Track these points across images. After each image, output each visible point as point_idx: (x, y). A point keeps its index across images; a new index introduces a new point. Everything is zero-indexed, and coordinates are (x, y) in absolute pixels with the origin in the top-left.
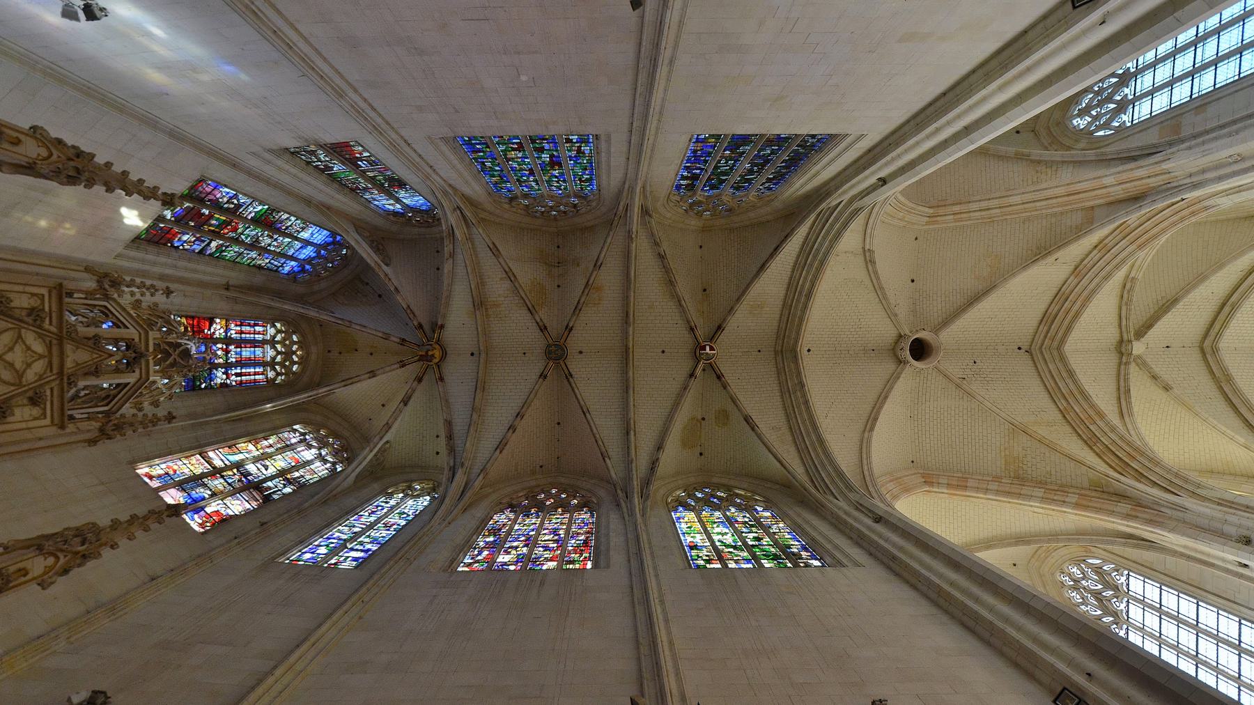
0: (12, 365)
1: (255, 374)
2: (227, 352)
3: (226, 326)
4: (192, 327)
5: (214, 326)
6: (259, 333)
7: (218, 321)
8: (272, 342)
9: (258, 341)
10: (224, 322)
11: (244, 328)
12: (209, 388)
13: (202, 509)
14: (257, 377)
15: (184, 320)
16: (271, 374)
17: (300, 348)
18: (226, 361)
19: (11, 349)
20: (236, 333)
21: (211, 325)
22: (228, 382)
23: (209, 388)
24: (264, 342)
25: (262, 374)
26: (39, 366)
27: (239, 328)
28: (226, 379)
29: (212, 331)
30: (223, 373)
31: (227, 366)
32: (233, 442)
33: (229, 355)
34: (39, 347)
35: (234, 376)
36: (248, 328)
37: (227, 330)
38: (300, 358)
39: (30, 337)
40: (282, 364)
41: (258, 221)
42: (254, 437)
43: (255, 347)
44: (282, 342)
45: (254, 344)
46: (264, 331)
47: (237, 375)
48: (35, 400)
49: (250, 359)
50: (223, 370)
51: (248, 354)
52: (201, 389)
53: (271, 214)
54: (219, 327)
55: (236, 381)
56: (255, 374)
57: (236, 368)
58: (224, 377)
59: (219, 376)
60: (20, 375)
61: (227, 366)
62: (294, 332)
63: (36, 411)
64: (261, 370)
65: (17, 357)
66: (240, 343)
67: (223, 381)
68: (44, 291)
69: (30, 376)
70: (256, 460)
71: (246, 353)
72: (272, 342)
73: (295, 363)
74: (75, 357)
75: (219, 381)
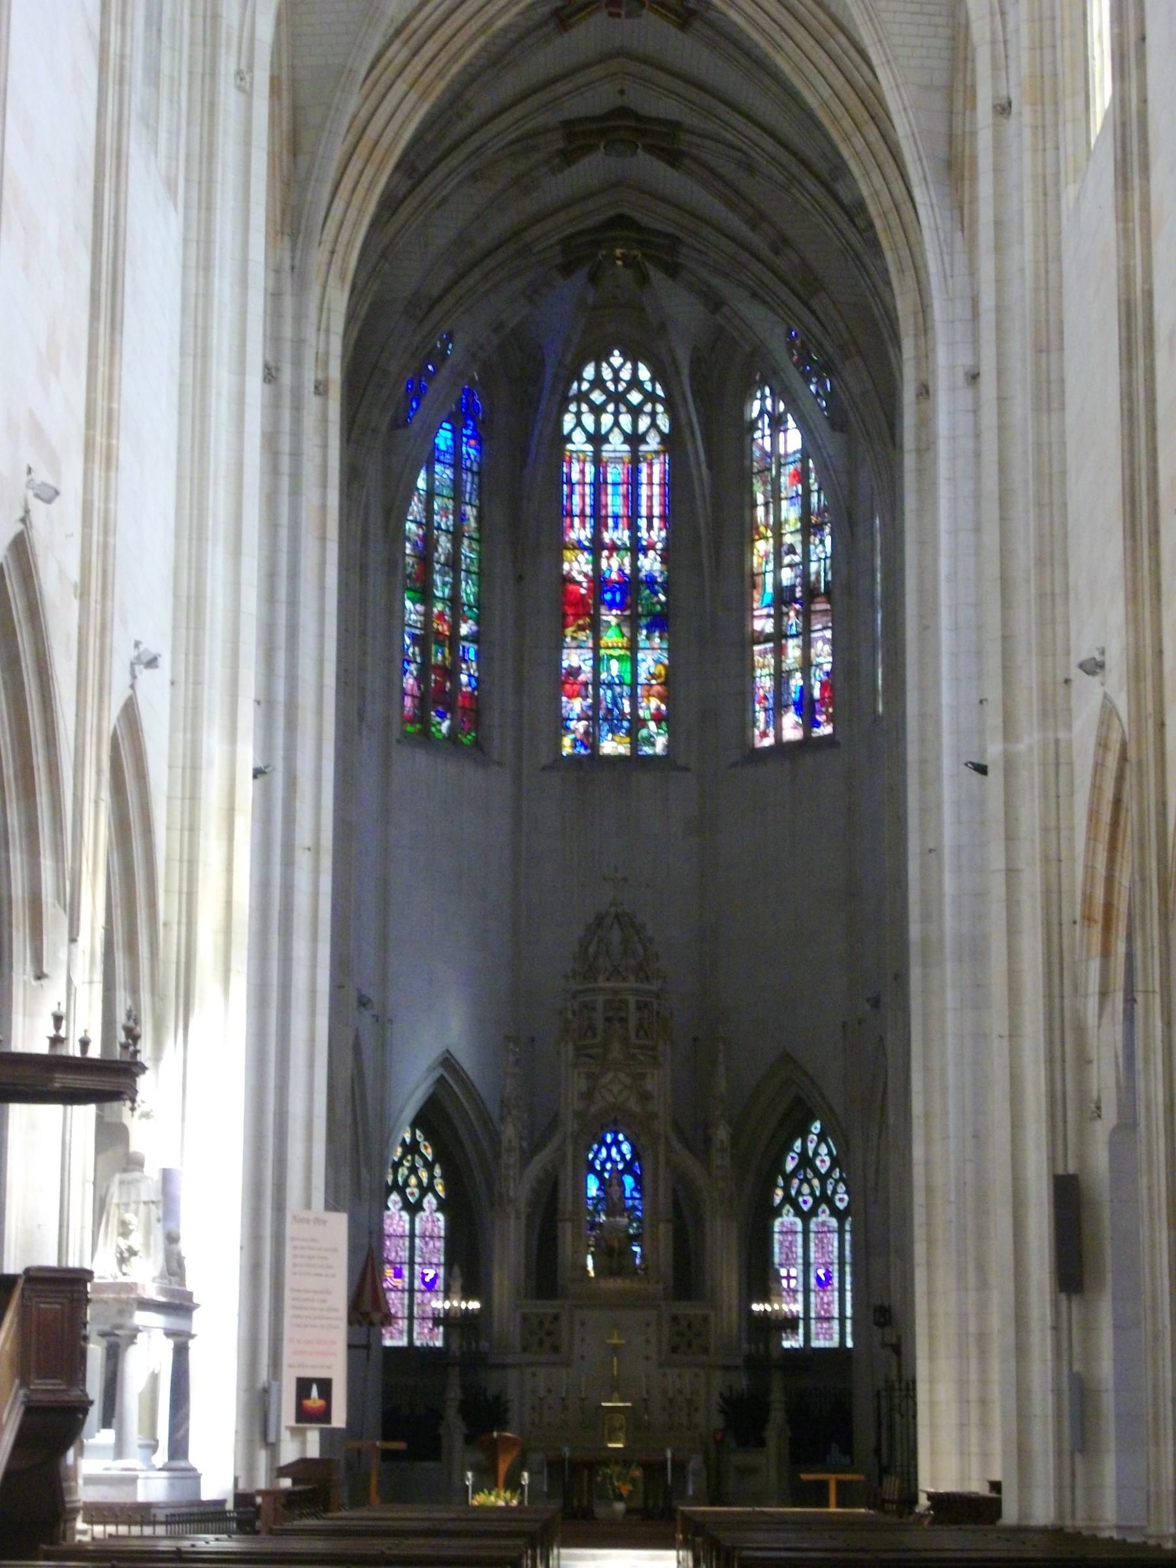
0: (620, 1092)
1: (650, 484)
2: (614, 548)
3: (574, 548)
4: (577, 616)
5: (574, 574)
6: (582, 472)
7: (566, 566)
8: (597, 439)
9: (597, 474)
10: (568, 554)
11: (576, 510)
12: (666, 587)
13: (813, 701)
15: (569, 631)
16: (653, 442)
17: (606, 356)
18: (626, 549)
19: (611, 1091)
20: (584, 528)
22: (659, 546)
23: (666, 587)
24: (597, 461)
25: (651, 465)
26: (621, 1075)
27: (577, 521)
28: (655, 550)
29: (580, 578)
30: (646, 556)
31: (637, 548)
32: (748, 580)
33: (619, 543)
34: (610, 1075)
35: (652, 533)
36: (576, 499)
37: (579, 546)
39: (604, 1081)
40: (635, 411)
41: (425, 596)
42: (749, 533)
43: (606, 482)
44: (597, 410)
45: (599, 485)
46: (578, 460)
47: (650, 527)
48: (643, 1076)
49: (625, 497)
50: (641, 556)
51: (619, 500)
52: (667, 603)
53: (409, 576)
54: (575, 565)
55: (660, 529)
56: (650, 484)
57: (638, 529)
58: (651, 553)
59: (650, 564)
60: (626, 1087)
61: (637, 548)
62: (580, 379)
63: (649, 1076)
64: (644, 467)
65: (616, 1089)
66: (599, 520)
67: (659, 559)
68: (576, 1071)
69: (628, 1081)
70: (779, 565)
71: (614, 503)
72: (597, 439)
73: (635, 370)
74: (616, 1052)
75: (657, 566)
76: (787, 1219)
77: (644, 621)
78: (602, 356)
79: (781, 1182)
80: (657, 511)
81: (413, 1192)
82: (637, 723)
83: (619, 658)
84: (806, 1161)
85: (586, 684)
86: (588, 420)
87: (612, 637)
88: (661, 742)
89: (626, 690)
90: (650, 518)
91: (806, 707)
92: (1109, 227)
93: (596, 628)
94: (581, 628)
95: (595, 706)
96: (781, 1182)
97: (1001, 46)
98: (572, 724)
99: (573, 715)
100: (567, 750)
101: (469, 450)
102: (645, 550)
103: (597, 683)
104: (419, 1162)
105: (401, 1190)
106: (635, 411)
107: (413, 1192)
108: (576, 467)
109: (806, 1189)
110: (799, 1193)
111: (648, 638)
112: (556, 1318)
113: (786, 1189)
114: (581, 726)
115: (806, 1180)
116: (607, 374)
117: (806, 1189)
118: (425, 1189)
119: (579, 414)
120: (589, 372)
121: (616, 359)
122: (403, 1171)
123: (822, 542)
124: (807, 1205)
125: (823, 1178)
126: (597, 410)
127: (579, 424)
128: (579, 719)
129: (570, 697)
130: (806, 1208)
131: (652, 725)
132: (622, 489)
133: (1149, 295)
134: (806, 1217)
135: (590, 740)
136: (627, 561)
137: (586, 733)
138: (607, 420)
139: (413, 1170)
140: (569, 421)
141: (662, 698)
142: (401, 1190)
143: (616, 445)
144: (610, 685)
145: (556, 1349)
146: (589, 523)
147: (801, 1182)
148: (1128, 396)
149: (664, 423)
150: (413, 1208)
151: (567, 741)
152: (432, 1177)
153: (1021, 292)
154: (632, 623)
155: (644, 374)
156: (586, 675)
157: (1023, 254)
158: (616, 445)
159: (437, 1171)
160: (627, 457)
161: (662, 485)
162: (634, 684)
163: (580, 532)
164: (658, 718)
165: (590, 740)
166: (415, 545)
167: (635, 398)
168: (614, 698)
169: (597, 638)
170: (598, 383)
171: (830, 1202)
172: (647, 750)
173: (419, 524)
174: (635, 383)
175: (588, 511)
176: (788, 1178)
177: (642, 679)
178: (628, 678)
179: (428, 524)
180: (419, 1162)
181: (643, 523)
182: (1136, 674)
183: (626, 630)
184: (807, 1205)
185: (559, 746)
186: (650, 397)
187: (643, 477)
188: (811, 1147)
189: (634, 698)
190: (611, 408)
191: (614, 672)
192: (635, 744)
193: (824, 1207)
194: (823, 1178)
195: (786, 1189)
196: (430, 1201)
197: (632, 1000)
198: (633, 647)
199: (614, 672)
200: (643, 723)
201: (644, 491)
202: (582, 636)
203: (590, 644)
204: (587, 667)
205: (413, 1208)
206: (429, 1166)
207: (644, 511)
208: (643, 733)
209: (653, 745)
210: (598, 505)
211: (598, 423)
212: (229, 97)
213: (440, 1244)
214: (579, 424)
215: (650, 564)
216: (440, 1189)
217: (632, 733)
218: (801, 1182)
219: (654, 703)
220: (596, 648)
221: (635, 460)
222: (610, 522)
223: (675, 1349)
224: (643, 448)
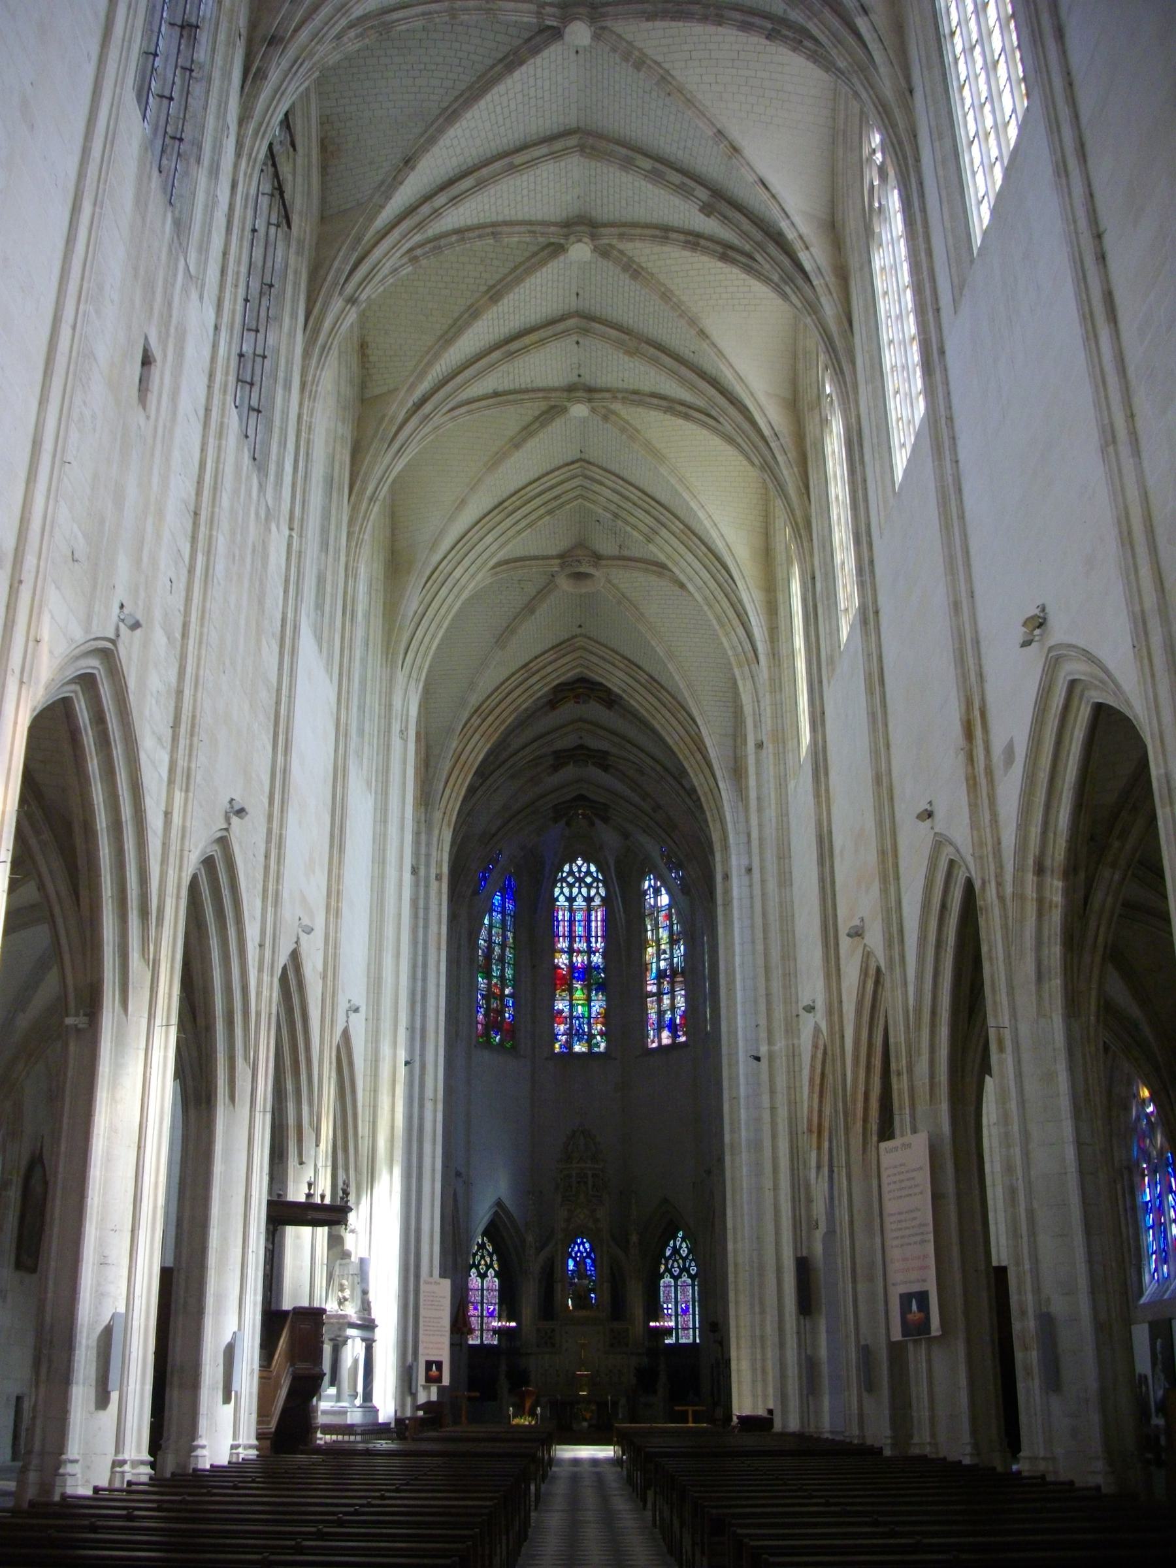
2: (579, 952)
4: (562, 985)
6: (564, 915)
7: (556, 961)
8: (571, 899)
10: (557, 955)
11: (561, 934)
12: (604, 970)
13: (676, 1025)
14: (599, 918)
16: (597, 901)
17: (575, 861)
21: (560, 968)
23: (604, 970)
24: (571, 910)
25: (597, 912)
27: (561, 939)
29: (563, 966)
31: (590, 951)
36: (561, 928)
37: (562, 951)
38: (584, 861)
40: (589, 886)
41: (488, 975)
42: (644, 944)
44: (571, 886)
45: (572, 921)
47: (596, 942)
49: (585, 927)
51: (581, 929)
52: (605, 978)
53: (480, 966)
57: (591, 942)
58: (597, 954)
59: (597, 959)
61: (590, 951)
64: (593, 913)
66: (572, 938)
70: (659, 960)
71: (579, 930)
72: (571, 899)
73: (588, 867)
75: (600, 960)
76: (667, 1279)
77: (594, 987)
78: (572, 860)
79: (663, 1261)
80: (599, 934)
81: (482, 1268)
82: (591, 1036)
83: (582, 1005)
84: (676, 1251)
85: (566, 1018)
86: (566, 891)
87: (579, 994)
88: (603, 1045)
89: (586, 1021)
90: (597, 937)
91: (673, 1027)
92: (810, 800)
93: (571, 991)
94: (563, 991)
95: (571, 1029)
96: (663, 1261)
97: (757, 715)
98: (560, 1037)
99: (560, 1033)
100: (557, 1050)
101: (510, 906)
102: (594, 953)
103: (571, 1017)
104: (485, 1253)
105: (477, 1267)
106: (589, 886)
107: (482, 1268)
108: (560, 913)
109: (676, 1265)
110: (672, 1267)
111: (596, 995)
112: (553, 1330)
113: (666, 1265)
114: (564, 1038)
115: (677, 1261)
116: (575, 869)
117: (676, 1265)
118: (489, 1267)
119: (562, 888)
120: (566, 868)
121: (580, 862)
122: (478, 1258)
123: (679, 948)
124: (676, 1271)
125: (684, 1259)
126: (571, 886)
127: (562, 892)
128: (563, 1035)
129: (559, 1024)
130: (676, 1274)
131: (599, 1038)
132: (583, 923)
133: (830, 832)
134: (676, 1278)
135: (569, 1045)
136: (585, 958)
137: (567, 1041)
138: (575, 891)
139: (483, 1257)
140: (557, 891)
141: (603, 1024)
142: (477, 1267)
143: (580, 902)
144: (578, 1018)
145: (553, 1345)
146: (567, 940)
147: (674, 1261)
148: (822, 880)
149: (602, 892)
150: (483, 1276)
151: (557, 1046)
152: (492, 1261)
153: (770, 831)
154: (588, 988)
155: (593, 868)
156: (566, 1013)
157: (771, 812)
158: (580, 902)
159: (495, 1258)
160: (585, 908)
161: (602, 921)
162: (590, 1017)
163: (563, 944)
164: (601, 1034)
165: (569, 1045)
166: (483, 951)
167: (589, 880)
168: (580, 1024)
169: (571, 995)
170: (571, 873)
171: (688, 1271)
172: (596, 1049)
173: (485, 941)
174: (589, 873)
175: (566, 934)
176: (667, 1259)
177: (593, 1015)
178: (586, 1014)
179: (489, 941)
180: (485, 1253)
181: (593, 940)
182: (830, 1013)
183: (585, 991)
184: (676, 1271)
185: (553, 1048)
186: (596, 879)
187: (593, 918)
188: (678, 1244)
189: (589, 1024)
190: (577, 885)
191: (580, 1012)
192: (590, 1047)
193: (685, 1273)
194: (684, 1259)
195: (666, 1265)
196: (491, 1272)
197: (590, 1173)
198: (589, 1000)
199: (580, 1012)
200: (594, 1036)
201: (593, 924)
202: (564, 994)
203: (568, 998)
204: (566, 1009)
205: (483, 1276)
206: (490, 1255)
207: (593, 934)
208: (594, 1041)
209: (599, 1047)
210: (571, 931)
211: (571, 892)
212: (396, 742)
213: (496, 1293)
214: (562, 892)
215: (597, 959)
216: (496, 1266)
217: (589, 1041)
218: (674, 1261)
219: (599, 1027)
220: (571, 1000)
221: (589, 909)
222: (577, 939)
223: (612, 1345)
224: (593, 904)
